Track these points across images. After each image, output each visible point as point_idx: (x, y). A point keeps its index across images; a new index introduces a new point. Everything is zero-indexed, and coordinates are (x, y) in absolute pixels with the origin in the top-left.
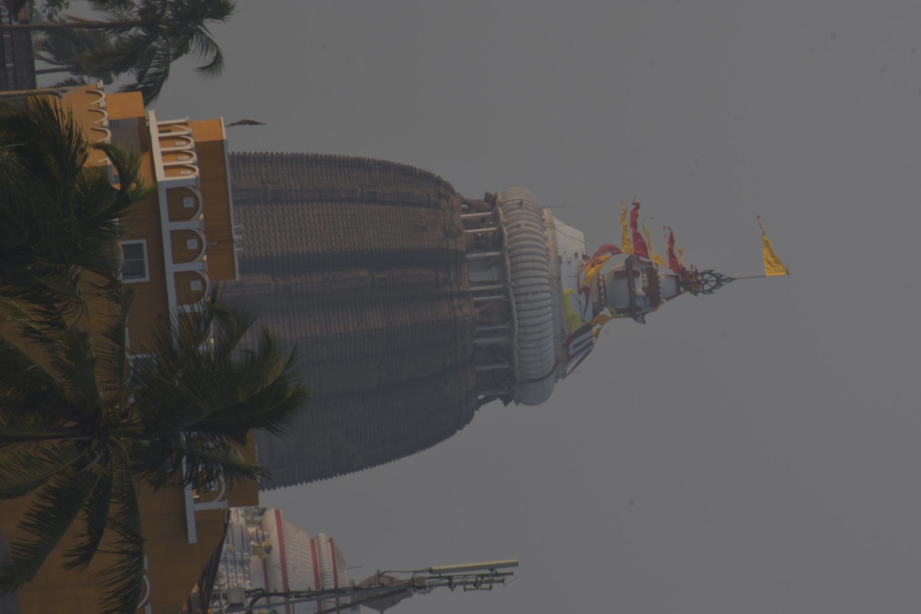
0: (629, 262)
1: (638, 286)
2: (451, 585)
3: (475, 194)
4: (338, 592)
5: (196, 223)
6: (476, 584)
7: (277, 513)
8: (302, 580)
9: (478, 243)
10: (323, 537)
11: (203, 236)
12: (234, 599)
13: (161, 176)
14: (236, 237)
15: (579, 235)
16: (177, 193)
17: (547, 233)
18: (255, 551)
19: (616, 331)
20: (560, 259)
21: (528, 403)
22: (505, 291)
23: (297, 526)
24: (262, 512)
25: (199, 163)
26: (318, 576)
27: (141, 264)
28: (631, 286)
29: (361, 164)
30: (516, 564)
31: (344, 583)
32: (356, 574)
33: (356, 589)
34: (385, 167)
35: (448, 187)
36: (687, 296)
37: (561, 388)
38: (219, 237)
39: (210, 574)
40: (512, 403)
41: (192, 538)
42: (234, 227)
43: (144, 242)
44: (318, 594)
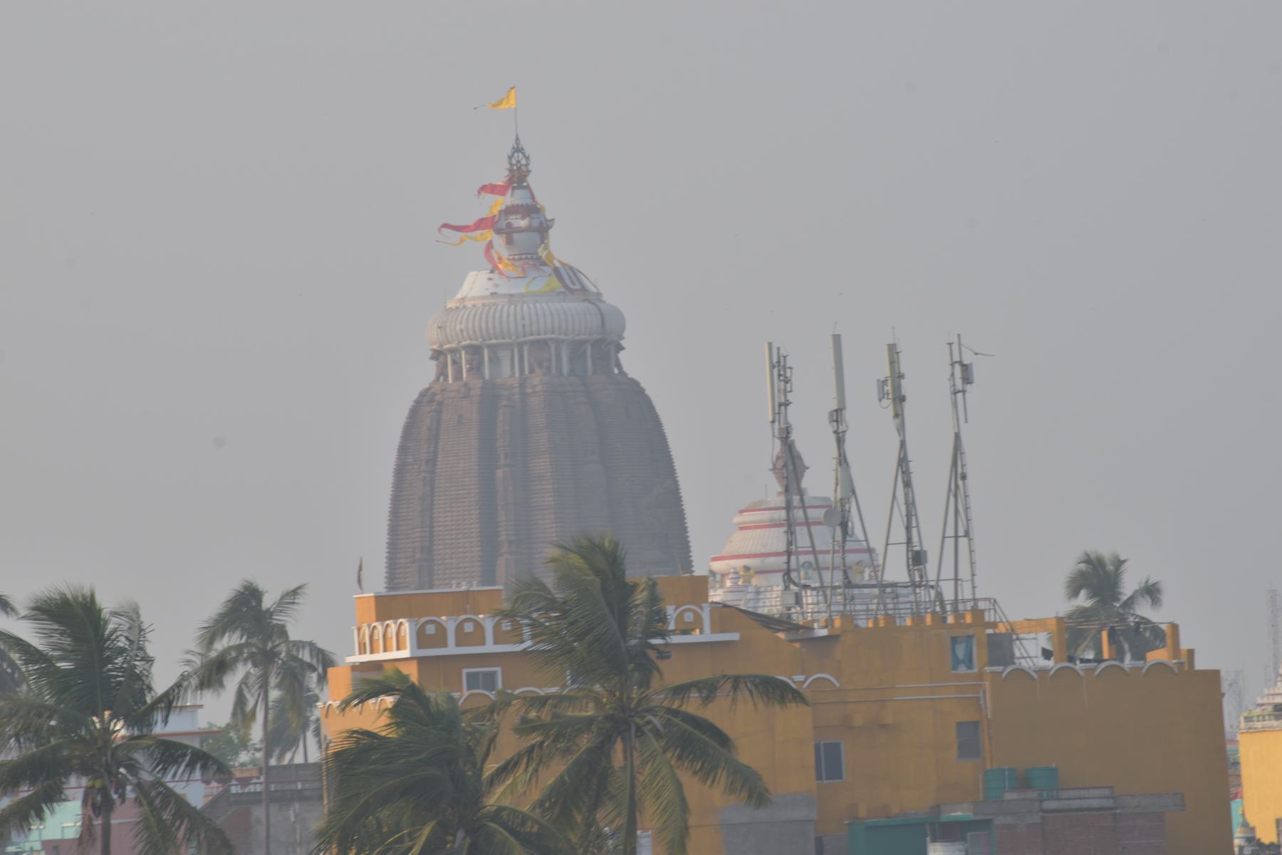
1: (521, 225)
2: (787, 404)
3: (432, 368)
4: (788, 507)
5: (450, 623)
6: (787, 381)
7: (715, 559)
8: (775, 540)
9: (476, 368)
10: (738, 519)
11: (462, 617)
13: (405, 653)
14: (464, 588)
15: (472, 274)
16: (422, 639)
17: (469, 304)
18: (747, 581)
19: (560, 246)
21: (623, 328)
22: (520, 345)
23: (729, 544)
24: (713, 573)
25: (395, 618)
26: (773, 525)
27: (485, 674)
28: (520, 230)
29: (400, 472)
30: (770, 345)
31: (781, 501)
32: (773, 491)
34: (403, 450)
35: (423, 394)
36: (531, 180)
38: (463, 602)
39: (767, 622)
40: (623, 343)
41: (735, 636)
42: (454, 589)
43: (465, 671)
44: (790, 526)
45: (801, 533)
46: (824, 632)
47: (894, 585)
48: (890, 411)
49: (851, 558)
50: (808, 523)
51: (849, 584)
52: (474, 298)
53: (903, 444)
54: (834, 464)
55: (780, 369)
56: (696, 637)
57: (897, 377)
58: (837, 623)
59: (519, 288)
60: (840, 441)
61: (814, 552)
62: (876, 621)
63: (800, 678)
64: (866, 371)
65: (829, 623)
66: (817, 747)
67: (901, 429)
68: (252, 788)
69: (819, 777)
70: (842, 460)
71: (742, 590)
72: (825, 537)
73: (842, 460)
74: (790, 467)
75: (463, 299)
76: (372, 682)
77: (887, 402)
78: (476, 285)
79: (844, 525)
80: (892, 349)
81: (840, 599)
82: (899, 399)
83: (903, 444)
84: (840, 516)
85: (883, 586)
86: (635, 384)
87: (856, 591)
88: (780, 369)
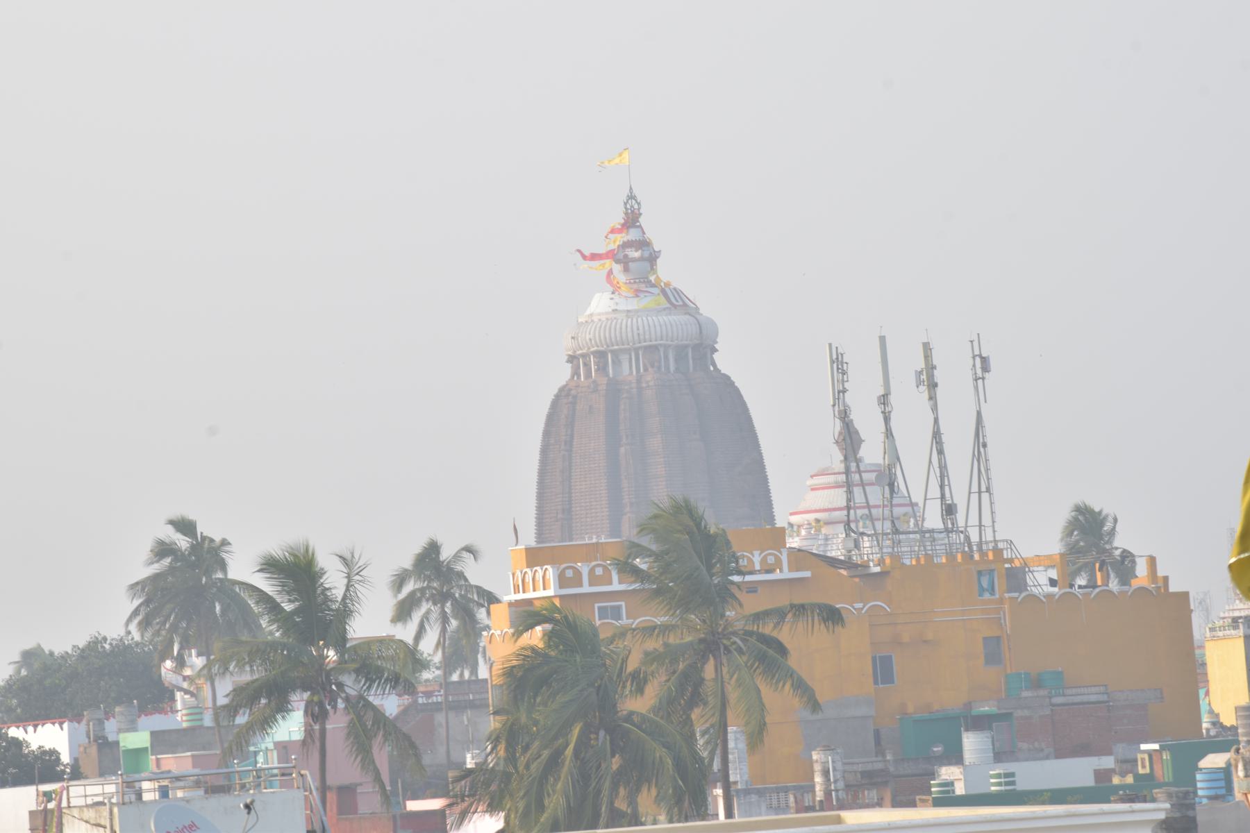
0: (618, 262)
1: (634, 255)
2: (844, 391)
3: (567, 370)
4: (847, 472)
5: (584, 569)
7: (791, 514)
9: (602, 368)
10: (810, 482)
11: (594, 563)
12: (851, 545)
13: (550, 592)
14: (594, 541)
15: (597, 295)
16: (562, 581)
17: (596, 319)
18: (818, 531)
19: (665, 271)
20: (615, 311)
22: (636, 350)
23: (803, 498)
24: (791, 525)
25: (542, 565)
26: (837, 486)
27: (612, 607)
28: (634, 260)
29: (545, 451)
30: (830, 345)
31: (841, 467)
32: (836, 459)
33: (846, 458)
34: (547, 434)
35: (561, 390)
37: (706, 311)
38: (593, 551)
39: (833, 562)
41: (807, 574)
43: (596, 605)
44: (849, 486)
45: (857, 491)
46: (878, 569)
47: (932, 531)
48: (926, 395)
49: (898, 511)
50: (863, 484)
51: (896, 531)
52: (599, 314)
53: (936, 420)
54: (882, 437)
55: (839, 364)
56: (777, 575)
57: (930, 368)
58: (888, 561)
59: (633, 304)
60: (887, 419)
61: (868, 507)
62: (918, 560)
63: (859, 605)
64: (907, 363)
65: (881, 562)
66: (874, 659)
67: (935, 408)
68: (435, 699)
69: (876, 682)
70: (889, 433)
71: (815, 538)
72: (876, 495)
73: (889, 433)
74: (849, 440)
75: (591, 315)
76: (526, 616)
77: (923, 388)
78: (601, 304)
79: (891, 486)
80: (927, 348)
81: (888, 543)
82: (933, 386)
83: (936, 420)
84: (888, 478)
85: (923, 532)
86: (727, 378)
87: (902, 537)
88: (839, 364)
